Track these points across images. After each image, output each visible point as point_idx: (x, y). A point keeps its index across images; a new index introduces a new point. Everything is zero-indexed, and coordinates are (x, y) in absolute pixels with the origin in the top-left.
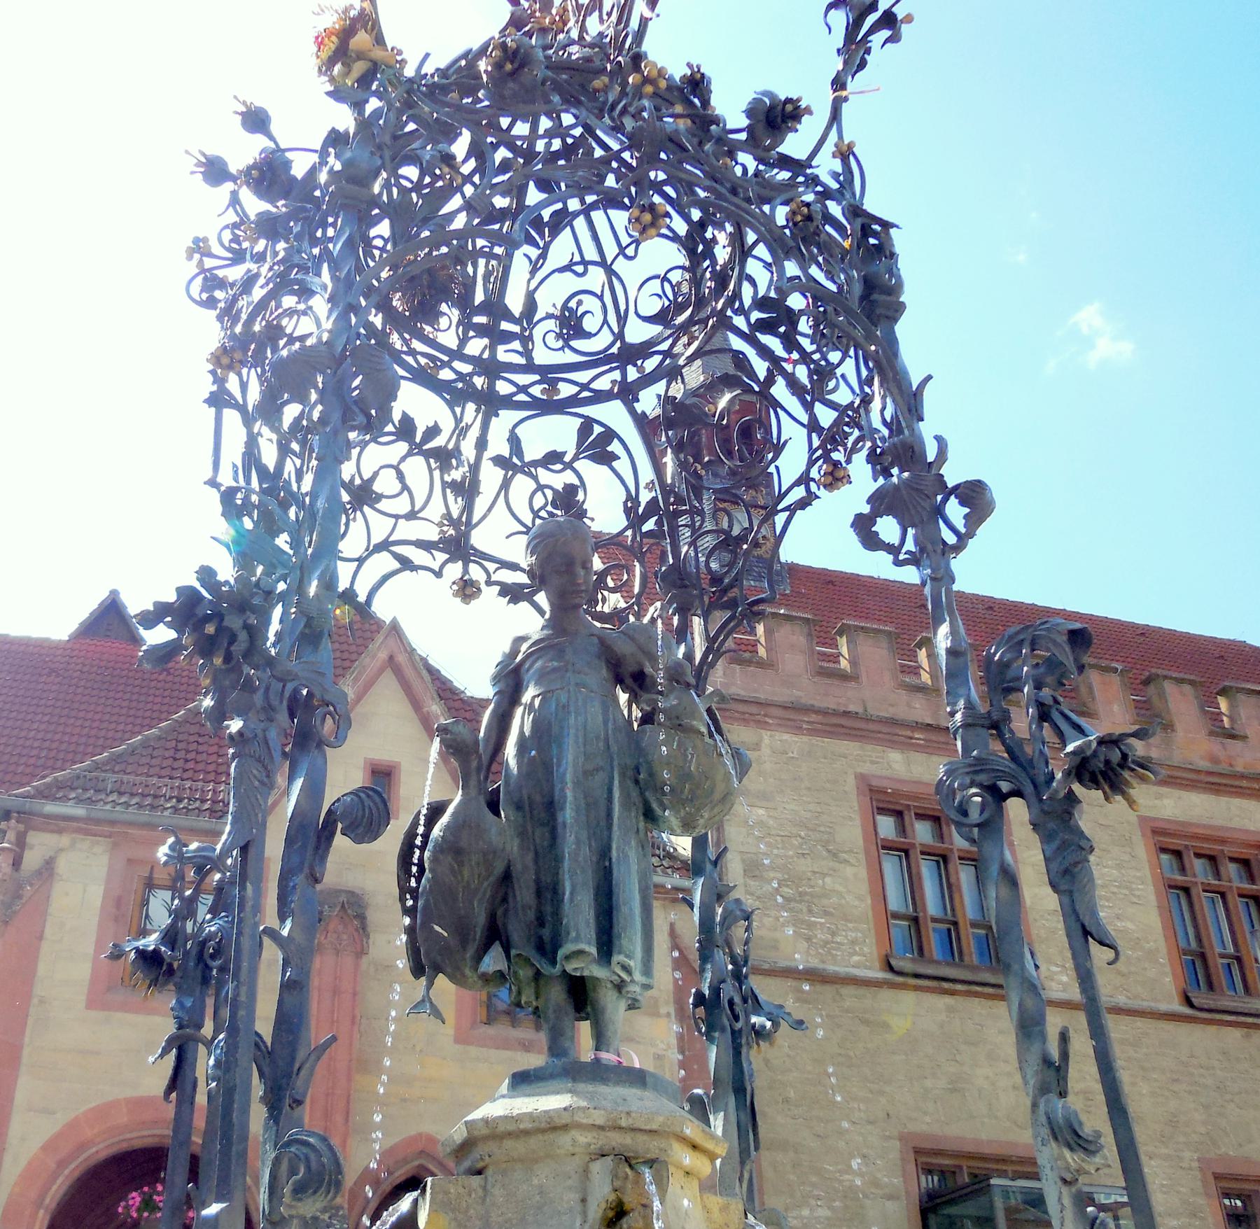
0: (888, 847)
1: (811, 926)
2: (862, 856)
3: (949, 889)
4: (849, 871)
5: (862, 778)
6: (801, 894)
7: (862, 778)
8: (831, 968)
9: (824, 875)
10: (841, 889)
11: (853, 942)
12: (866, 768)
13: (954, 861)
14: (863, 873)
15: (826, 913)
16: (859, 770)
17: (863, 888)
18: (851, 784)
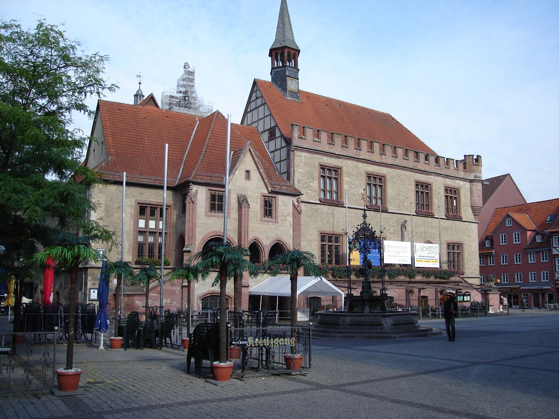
0: (322, 176)
1: (308, 193)
2: (317, 179)
3: (331, 185)
4: (315, 182)
5: (319, 163)
6: (307, 186)
7: (319, 163)
8: (311, 201)
9: (311, 183)
10: (313, 185)
11: (315, 196)
12: (320, 161)
13: (332, 179)
14: (317, 182)
15: (311, 190)
16: (319, 161)
17: (317, 185)
18: (317, 164)
